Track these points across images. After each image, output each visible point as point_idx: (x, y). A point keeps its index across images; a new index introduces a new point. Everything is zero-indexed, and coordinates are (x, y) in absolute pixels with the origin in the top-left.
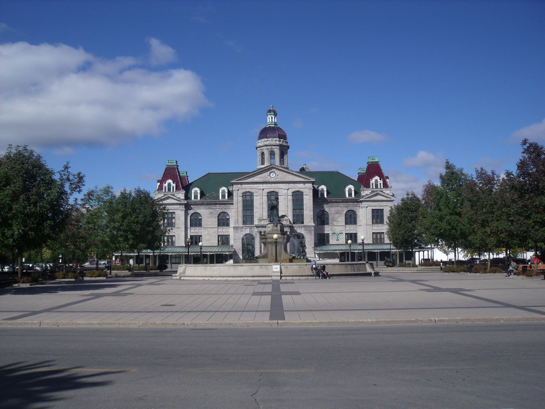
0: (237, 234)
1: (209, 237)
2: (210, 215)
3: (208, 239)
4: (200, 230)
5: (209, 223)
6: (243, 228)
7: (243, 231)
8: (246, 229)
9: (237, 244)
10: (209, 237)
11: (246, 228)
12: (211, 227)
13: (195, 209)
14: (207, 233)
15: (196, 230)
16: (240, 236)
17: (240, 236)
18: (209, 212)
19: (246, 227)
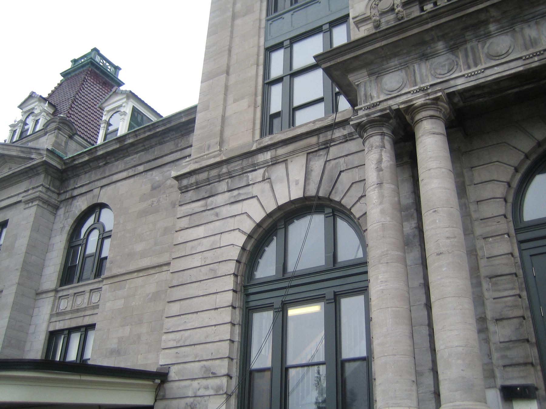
0: (200, 232)
1: (126, 331)
2: (150, 202)
3: (121, 340)
4: (95, 298)
5: (139, 247)
6: (255, 168)
7: (255, 190)
8: (279, 171)
9: (194, 321)
10: (126, 331)
11: (275, 162)
12: (146, 262)
13: (96, 191)
14: (120, 303)
15: (79, 300)
16: (226, 239)
17: (226, 239)
18: (147, 188)
19: (281, 151)
